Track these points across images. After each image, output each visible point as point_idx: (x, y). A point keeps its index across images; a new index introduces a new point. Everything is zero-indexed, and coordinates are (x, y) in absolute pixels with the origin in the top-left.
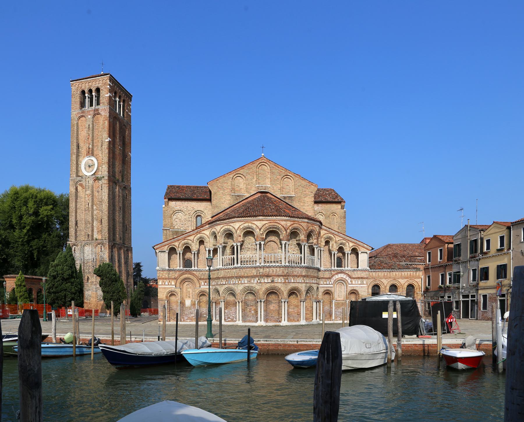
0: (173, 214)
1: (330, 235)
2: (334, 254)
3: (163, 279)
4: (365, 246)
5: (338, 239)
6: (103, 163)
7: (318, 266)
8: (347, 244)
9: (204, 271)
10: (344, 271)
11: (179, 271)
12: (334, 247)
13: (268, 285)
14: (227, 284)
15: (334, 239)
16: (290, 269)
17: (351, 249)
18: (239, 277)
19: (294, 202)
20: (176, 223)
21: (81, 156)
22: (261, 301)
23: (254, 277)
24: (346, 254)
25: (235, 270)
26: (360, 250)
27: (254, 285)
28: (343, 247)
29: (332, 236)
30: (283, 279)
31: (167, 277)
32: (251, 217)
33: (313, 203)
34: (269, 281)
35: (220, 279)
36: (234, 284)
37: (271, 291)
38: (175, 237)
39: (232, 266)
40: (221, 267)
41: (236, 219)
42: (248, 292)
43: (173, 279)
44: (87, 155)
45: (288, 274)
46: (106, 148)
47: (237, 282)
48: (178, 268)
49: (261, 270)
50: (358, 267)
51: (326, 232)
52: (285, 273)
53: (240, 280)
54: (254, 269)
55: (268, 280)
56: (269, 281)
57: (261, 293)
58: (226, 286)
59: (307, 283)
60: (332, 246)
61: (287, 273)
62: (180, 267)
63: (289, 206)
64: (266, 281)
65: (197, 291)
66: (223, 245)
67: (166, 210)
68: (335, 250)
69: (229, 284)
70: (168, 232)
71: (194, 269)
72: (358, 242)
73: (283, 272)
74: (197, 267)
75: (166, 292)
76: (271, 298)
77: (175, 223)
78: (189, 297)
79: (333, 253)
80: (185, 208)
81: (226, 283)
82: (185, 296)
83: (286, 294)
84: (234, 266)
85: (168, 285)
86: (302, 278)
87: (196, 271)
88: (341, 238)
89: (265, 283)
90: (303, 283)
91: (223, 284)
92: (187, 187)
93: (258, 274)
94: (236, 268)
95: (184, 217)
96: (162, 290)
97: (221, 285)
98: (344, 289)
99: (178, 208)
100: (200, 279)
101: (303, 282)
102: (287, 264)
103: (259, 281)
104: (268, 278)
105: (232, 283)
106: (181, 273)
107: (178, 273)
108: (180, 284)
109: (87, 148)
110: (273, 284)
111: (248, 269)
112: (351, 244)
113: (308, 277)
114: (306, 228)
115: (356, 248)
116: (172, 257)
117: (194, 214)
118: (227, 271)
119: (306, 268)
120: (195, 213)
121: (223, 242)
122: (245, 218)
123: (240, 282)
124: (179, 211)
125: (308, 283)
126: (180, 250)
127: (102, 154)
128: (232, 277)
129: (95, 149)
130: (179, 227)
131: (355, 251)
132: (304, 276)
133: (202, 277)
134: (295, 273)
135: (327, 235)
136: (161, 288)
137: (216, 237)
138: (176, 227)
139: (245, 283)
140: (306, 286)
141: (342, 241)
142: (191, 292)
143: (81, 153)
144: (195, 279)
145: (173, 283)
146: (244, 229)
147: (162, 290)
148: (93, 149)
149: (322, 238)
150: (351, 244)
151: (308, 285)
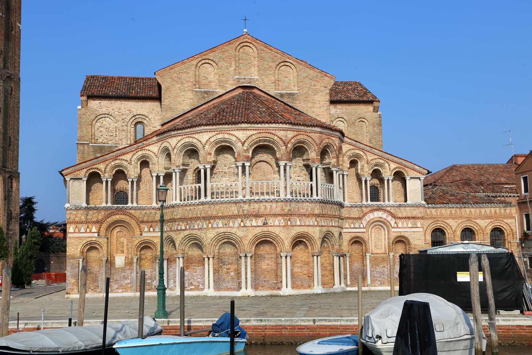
0: (96, 120)
1: (357, 151)
2: (366, 181)
3: (77, 223)
4: (417, 167)
5: (370, 157)
7: (340, 200)
8: (387, 165)
9: (149, 209)
10: (383, 207)
11: (106, 209)
12: (366, 171)
13: (258, 231)
14: (188, 230)
15: (365, 157)
16: (293, 204)
17: (394, 172)
18: (208, 218)
19: (297, 102)
20: (100, 134)
22: (246, 256)
23: (234, 217)
24: (386, 182)
25: (201, 207)
26: (409, 174)
27: (233, 231)
28: (380, 169)
29: (361, 153)
30: (282, 220)
31: (84, 220)
32: (228, 125)
33: (328, 103)
34: (260, 223)
35: (175, 221)
36: (200, 229)
37: (263, 239)
38: (99, 155)
39: (197, 201)
40: (178, 201)
41: (203, 128)
42: (223, 241)
43: (94, 223)
45: (290, 213)
47: (205, 226)
48: (104, 205)
49: (246, 207)
50: (406, 201)
51: (351, 147)
52: (286, 211)
53: (210, 223)
54: (233, 205)
55: (257, 223)
56: (261, 224)
57: (246, 242)
58: (187, 233)
59: (323, 226)
60: (362, 169)
61: (289, 210)
62: (107, 203)
63: (290, 109)
64: (254, 223)
65: (137, 242)
66: (181, 167)
67: (84, 114)
68: (366, 174)
69: (192, 229)
70: (86, 148)
71: (131, 205)
72: (404, 162)
73: (283, 210)
74: (137, 203)
75: (82, 244)
76: (262, 250)
77: (98, 134)
78: (123, 252)
79: (363, 179)
80: (117, 110)
81: (186, 228)
82: (115, 251)
83: (287, 244)
84: (200, 201)
85: (86, 232)
86: (314, 218)
87: (135, 209)
88: (376, 157)
89: (252, 226)
90: (316, 226)
91: (181, 230)
92: (119, 78)
93: (241, 213)
94: (203, 204)
95: (113, 125)
96: (73, 241)
97: (178, 230)
98: (385, 236)
99: (104, 110)
100: (142, 222)
101: (316, 224)
102: (289, 196)
103: (242, 224)
104: (258, 218)
105: (196, 227)
106: (108, 212)
107: (103, 213)
108: (107, 230)
110: (265, 229)
111: (223, 205)
112: (393, 166)
113: (323, 217)
114: (318, 142)
115: (402, 170)
116: (93, 188)
117: (131, 121)
118: (188, 208)
119: (320, 202)
120: (133, 118)
121: (181, 162)
122: (217, 127)
123: (210, 226)
124: (106, 116)
125: (325, 226)
126: (107, 176)
128: (197, 219)
130: (105, 141)
131: (399, 176)
132: (318, 216)
133: (145, 219)
134: (302, 211)
135: (353, 151)
136: (73, 237)
137: (169, 155)
138: (100, 140)
139: (219, 228)
140: (321, 231)
141: (378, 160)
142: (125, 244)
144: (133, 223)
145: (94, 230)
146: (217, 143)
147: (73, 241)
149: (345, 157)
150: (393, 166)
151: (325, 229)
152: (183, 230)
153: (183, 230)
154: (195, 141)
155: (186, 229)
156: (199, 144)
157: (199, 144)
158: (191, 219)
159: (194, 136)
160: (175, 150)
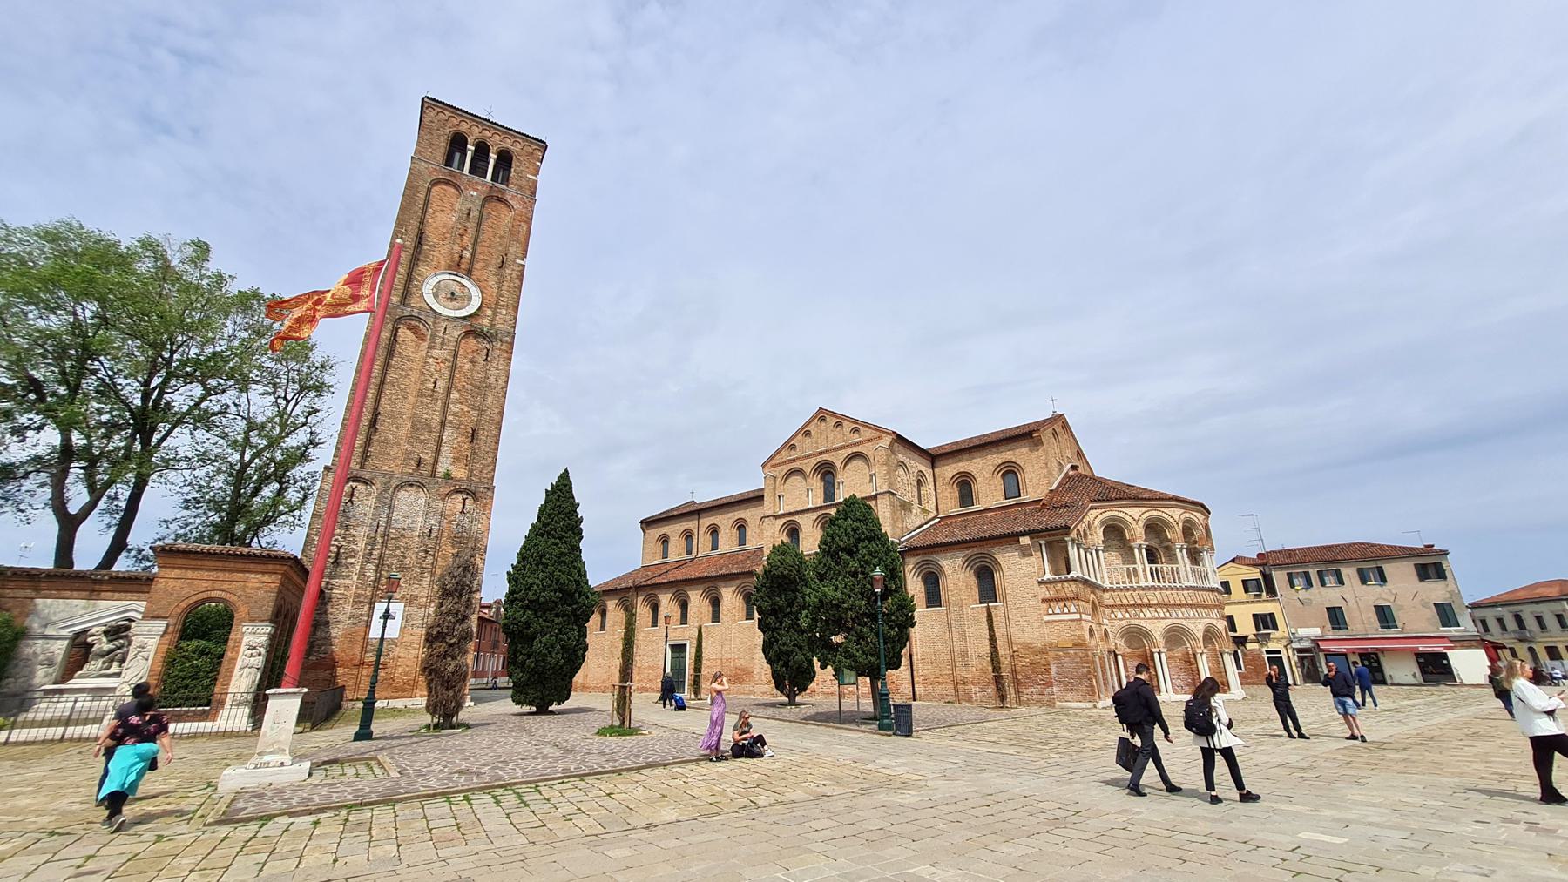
6: (502, 303)
21: (424, 262)
27: (1214, 622)
36: (1187, 618)
40: (1150, 583)
44: (450, 267)
46: (514, 276)
58: (1169, 622)
91: (1159, 618)
94: (1188, 588)
105: (1181, 616)
109: (452, 254)
118: (1168, 592)
127: (500, 282)
129: (477, 266)
143: (429, 258)
148: (471, 264)
152: (1163, 618)
153: (1163, 618)
154: (1166, 516)
155: (1166, 618)
156: (1171, 520)
157: (1171, 520)
158: (1173, 606)
159: (1162, 509)
160: (1140, 522)
